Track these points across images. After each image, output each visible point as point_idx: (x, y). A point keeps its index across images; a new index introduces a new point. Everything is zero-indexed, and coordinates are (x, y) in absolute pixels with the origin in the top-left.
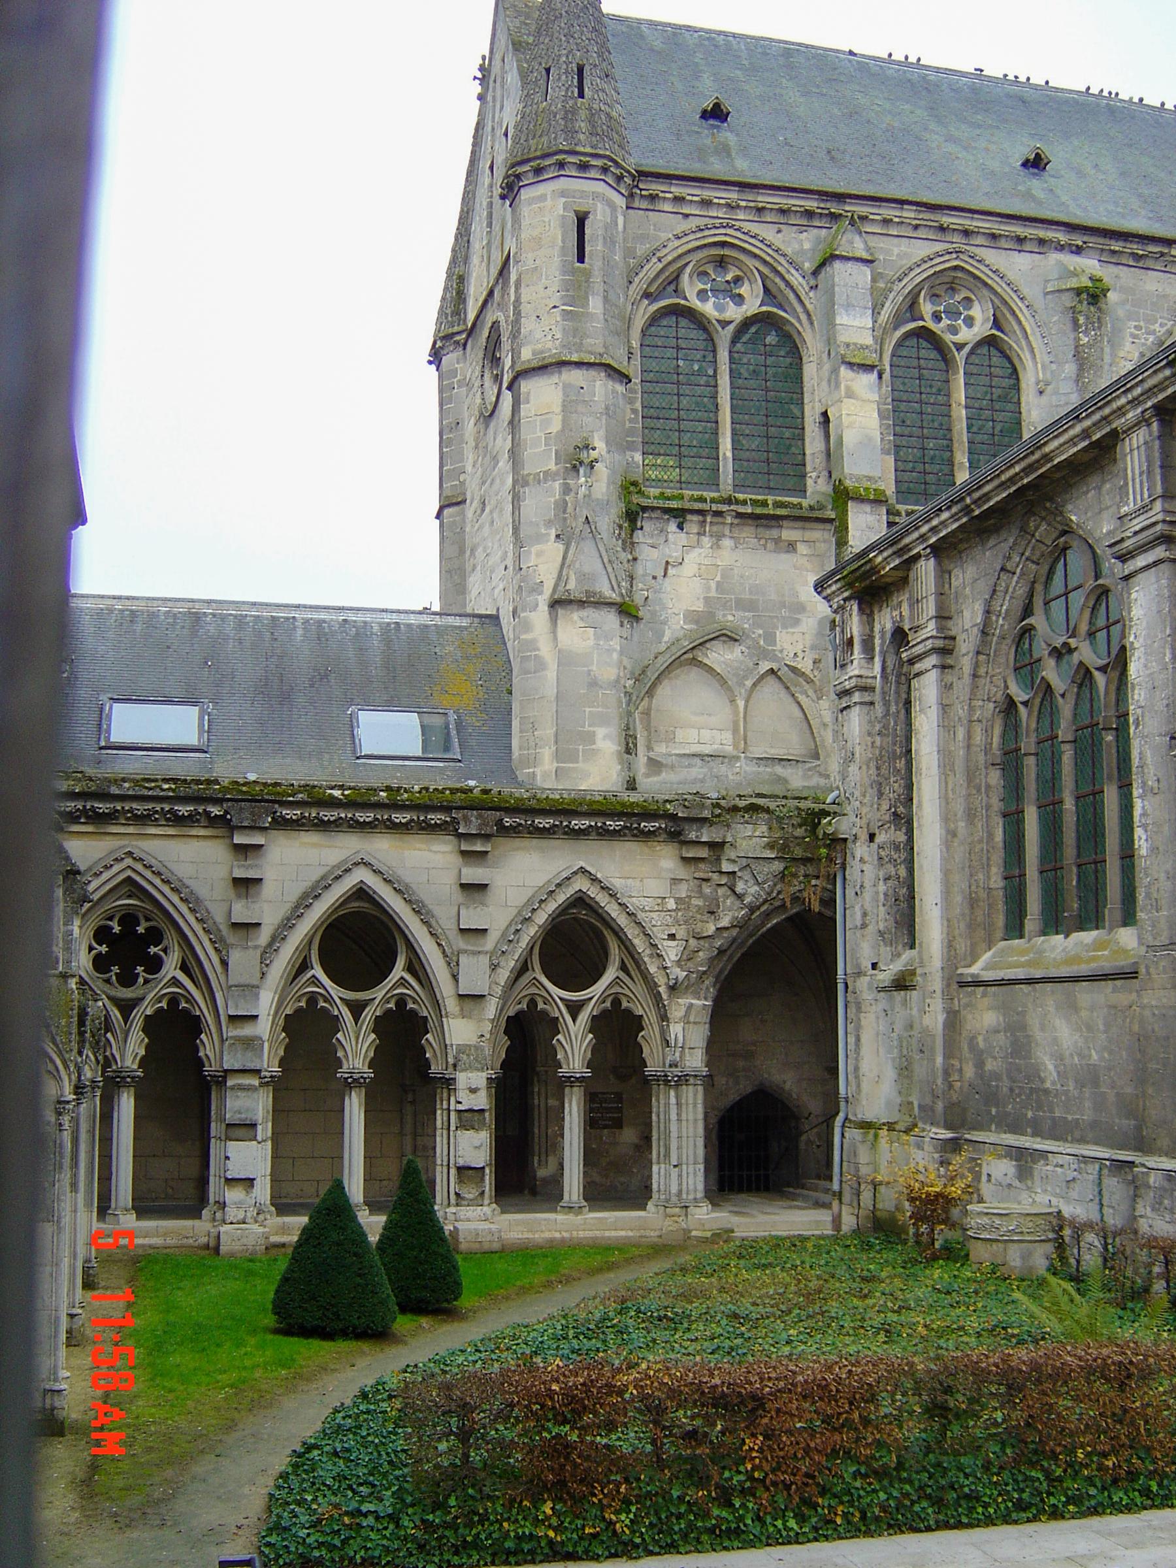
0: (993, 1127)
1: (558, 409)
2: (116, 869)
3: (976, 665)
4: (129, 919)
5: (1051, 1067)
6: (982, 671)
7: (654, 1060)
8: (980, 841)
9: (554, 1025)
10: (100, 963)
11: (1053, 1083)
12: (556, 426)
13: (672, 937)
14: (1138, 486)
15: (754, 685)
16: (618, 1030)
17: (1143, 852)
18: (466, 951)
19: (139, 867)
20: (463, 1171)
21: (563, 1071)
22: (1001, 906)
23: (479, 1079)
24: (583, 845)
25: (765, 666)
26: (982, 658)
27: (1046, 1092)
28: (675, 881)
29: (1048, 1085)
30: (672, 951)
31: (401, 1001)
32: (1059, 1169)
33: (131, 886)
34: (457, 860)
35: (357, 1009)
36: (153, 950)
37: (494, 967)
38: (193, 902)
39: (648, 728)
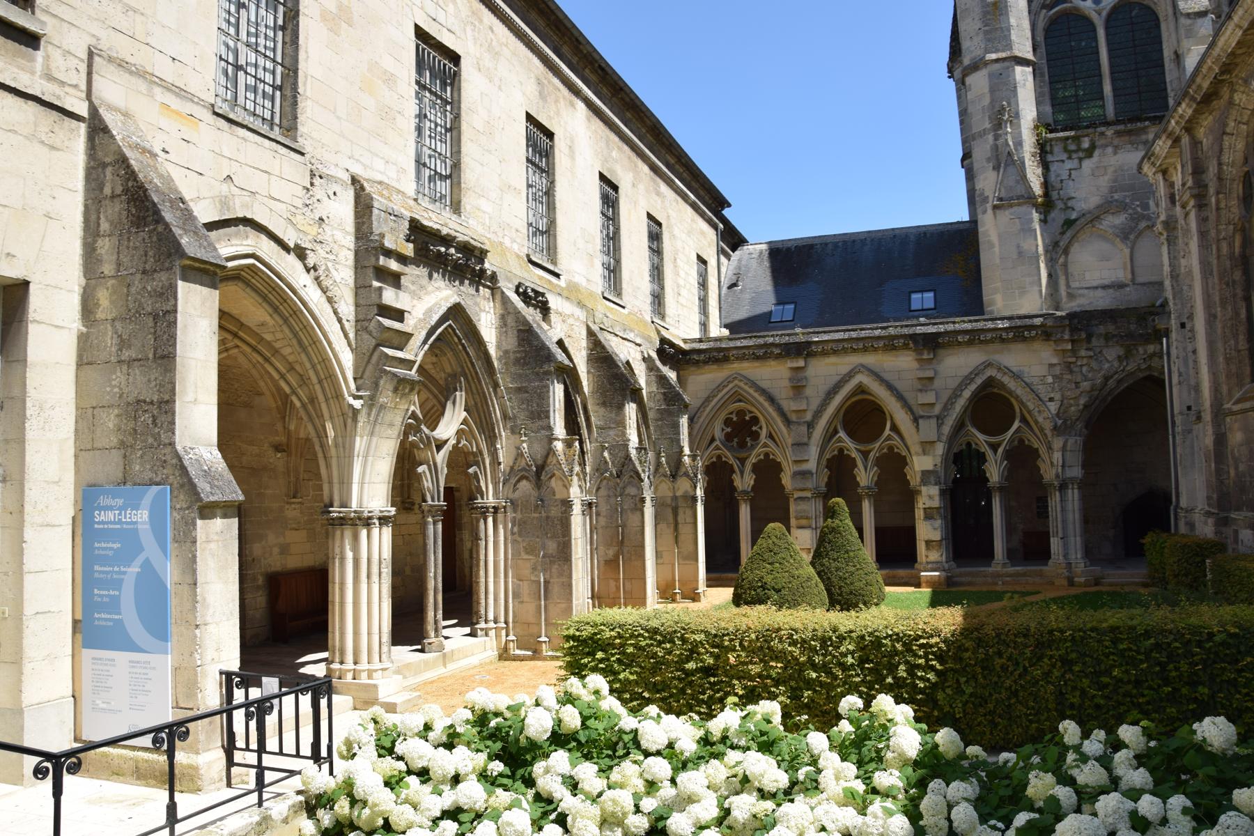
1: (986, 90)
2: (731, 386)
3: (1218, 202)
4: (741, 413)
6: (1222, 205)
7: (1049, 473)
9: (982, 458)
10: (728, 438)
12: (987, 101)
13: (1051, 399)
15: (1137, 237)
16: (1022, 458)
18: (922, 417)
19: (742, 384)
20: (928, 543)
21: (989, 484)
22: (1247, 361)
23: (934, 491)
24: (991, 347)
25: (1143, 224)
26: (1221, 196)
28: (1051, 365)
30: (1053, 407)
31: (891, 448)
33: (737, 397)
34: (915, 365)
35: (865, 454)
36: (754, 428)
37: (939, 426)
38: (772, 400)
39: (1067, 274)
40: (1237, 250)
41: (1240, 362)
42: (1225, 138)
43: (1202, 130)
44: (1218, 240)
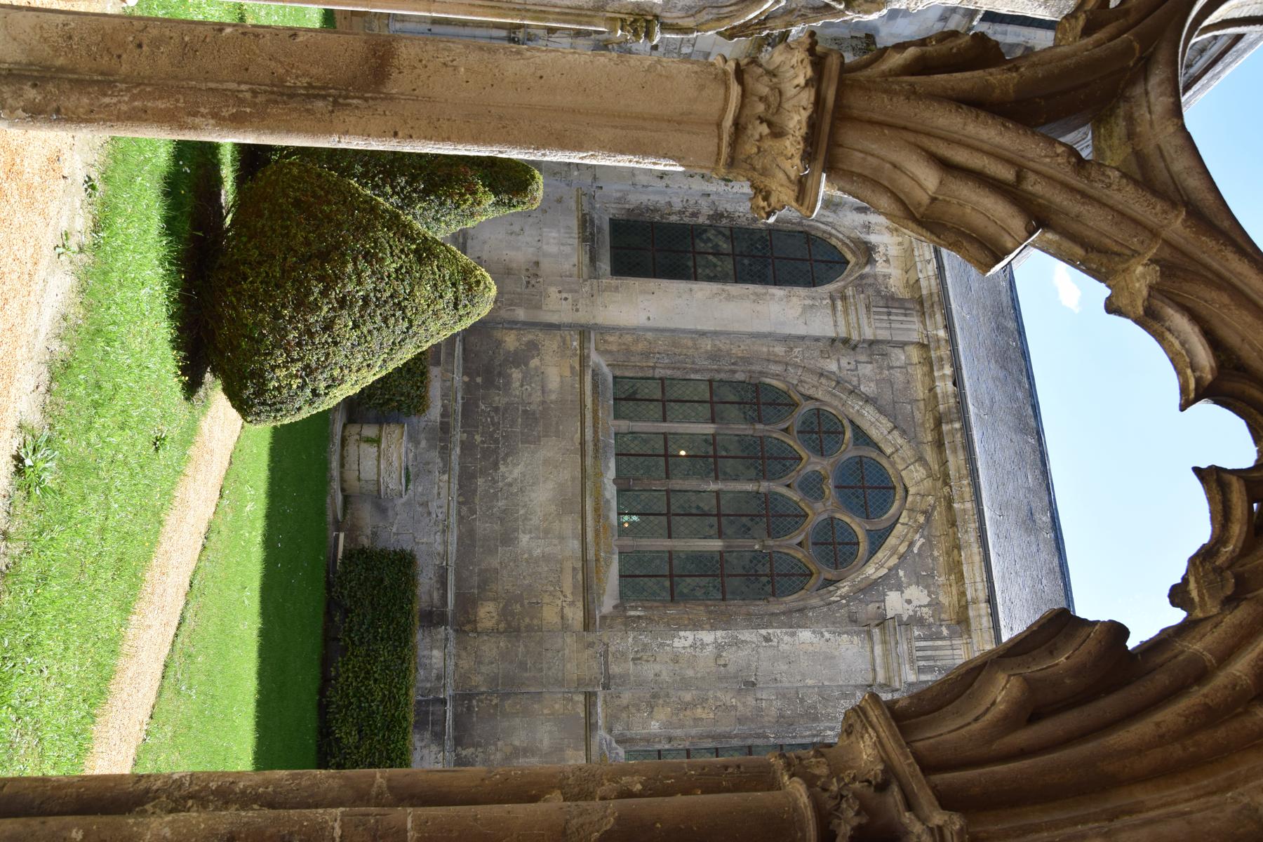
0: (466, 379)
5: (517, 472)
6: (823, 380)
8: (693, 363)
11: (504, 477)
14: (929, 653)
17: (677, 643)
26: (834, 384)
27: (496, 466)
29: (502, 468)
32: (435, 491)
40: (768, 381)
41: (642, 368)
42: (890, 425)
43: (915, 360)
44: (787, 364)
